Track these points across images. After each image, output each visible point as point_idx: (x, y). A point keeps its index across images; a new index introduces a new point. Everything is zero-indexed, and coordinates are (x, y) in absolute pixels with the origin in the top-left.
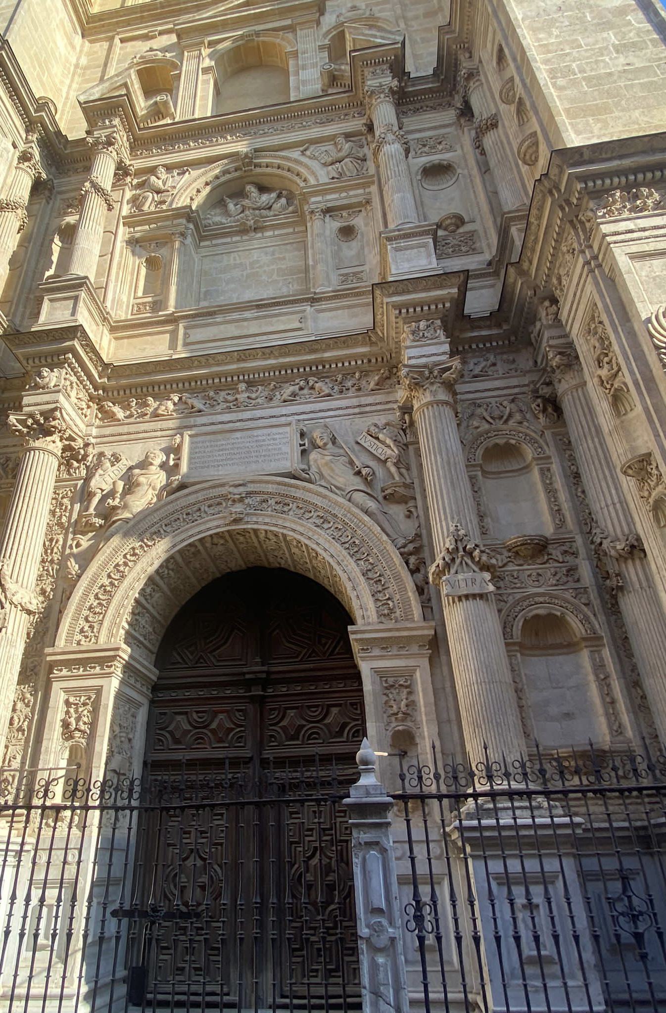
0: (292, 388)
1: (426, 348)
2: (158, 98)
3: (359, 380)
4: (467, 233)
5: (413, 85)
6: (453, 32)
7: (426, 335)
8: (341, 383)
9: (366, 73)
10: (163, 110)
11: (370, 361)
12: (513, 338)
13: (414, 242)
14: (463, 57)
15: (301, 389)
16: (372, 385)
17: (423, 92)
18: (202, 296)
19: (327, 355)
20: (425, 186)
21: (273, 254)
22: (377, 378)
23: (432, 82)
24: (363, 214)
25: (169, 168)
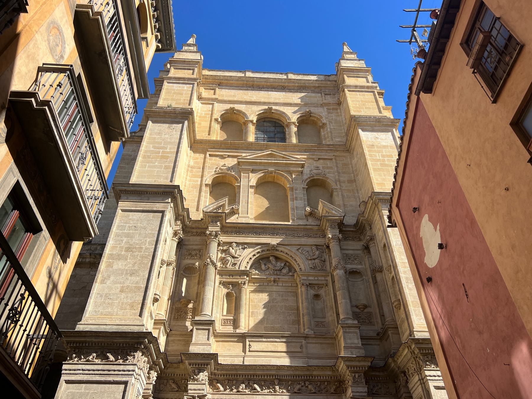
0: (298, 387)
1: (359, 388)
2: (234, 207)
3: (327, 386)
4: (368, 313)
5: (345, 228)
6: (364, 217)
7: (358, 380)
8: (319, 386)
9: (328, 224)
10: (235, 211)
11: (331, 377)
12: (388, 378)
13: (352, 330)
14: (368, 228)
15: (302, 386)
16: (332, 391)
17: (349, 231)
18: (250, 314)
19: (315, 373)
20: (349, 279)
21: (282, 297)
22: (334, 387)
23: (353, 228)
24: (323, 290)
25: (238, 244)
